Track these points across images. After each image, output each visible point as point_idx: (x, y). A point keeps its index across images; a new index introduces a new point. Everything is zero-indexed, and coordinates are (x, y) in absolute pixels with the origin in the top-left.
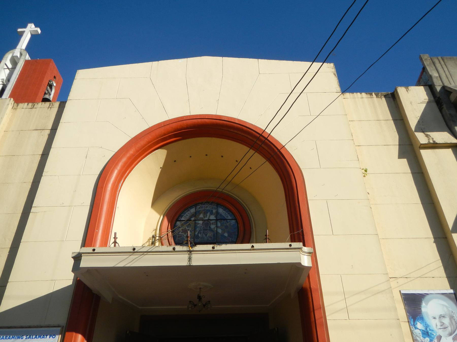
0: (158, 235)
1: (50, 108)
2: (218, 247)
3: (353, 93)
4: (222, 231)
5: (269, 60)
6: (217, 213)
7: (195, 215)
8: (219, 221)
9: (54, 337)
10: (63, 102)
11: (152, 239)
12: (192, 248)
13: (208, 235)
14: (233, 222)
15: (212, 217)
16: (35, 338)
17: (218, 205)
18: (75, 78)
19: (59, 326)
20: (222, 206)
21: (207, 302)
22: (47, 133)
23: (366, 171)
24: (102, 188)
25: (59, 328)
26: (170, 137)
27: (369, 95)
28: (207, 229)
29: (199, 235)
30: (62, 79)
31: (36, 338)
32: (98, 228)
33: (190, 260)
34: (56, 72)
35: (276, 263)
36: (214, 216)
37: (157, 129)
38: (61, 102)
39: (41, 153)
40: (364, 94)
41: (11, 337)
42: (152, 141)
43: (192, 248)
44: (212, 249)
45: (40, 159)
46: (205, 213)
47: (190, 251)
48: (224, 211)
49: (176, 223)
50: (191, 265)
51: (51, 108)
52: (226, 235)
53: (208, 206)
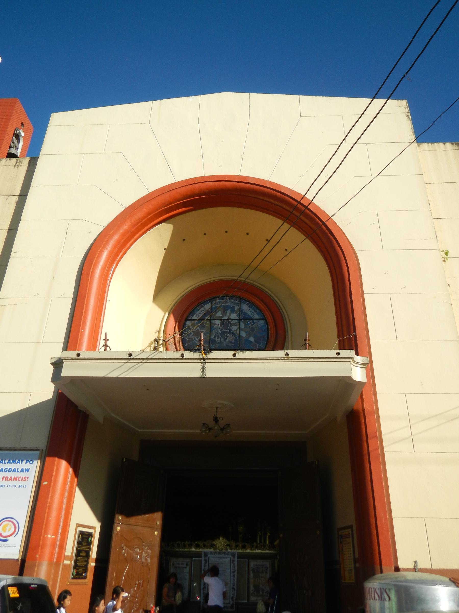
0: (162, 339)
1: (16, 167)
2: (240, 354)
3: (433, 144)
4: (246, 335)
5: (314, 97)
6: (240, 310)
7: (211, 312)
8: (242, 321)
9: (31, 462)
10: (33, 157)
11: (155, 343)
12: (206, 354)
13: (227, 340)
14: (262, 322)
15: (234, 316)
16: (8, 463)
17: (241, 299)
18: (49, 125)
19: (37, 450)
20: (247, 301)
21: (226, 425)
22: (15, 201)
23: (447, 254)
24: (88, 274)
25: (38, 452)
26: (177, 207)
27: (456, 146)
28: (228, 331)
29: (216, 339)
30: (32, 127)
31: (10, 463)
32: (84, 328)
33: (203, 370)
34: (24, 117)
35: (319, 376)
36: (236, 314)
37: (160, 195)
38: (31, 158)
39: (7, 227)
40: (448, 145)
42: (153, 212)
43: (206, 354)
44: (233, 357)
45: (6, 235)
46: (224, 310)
47: (204, 359)
48: (249, 308)
49: (185, 323)
50: (205, 376)
51: (18, 166)
52: (252, 339)
53: (228, 302)
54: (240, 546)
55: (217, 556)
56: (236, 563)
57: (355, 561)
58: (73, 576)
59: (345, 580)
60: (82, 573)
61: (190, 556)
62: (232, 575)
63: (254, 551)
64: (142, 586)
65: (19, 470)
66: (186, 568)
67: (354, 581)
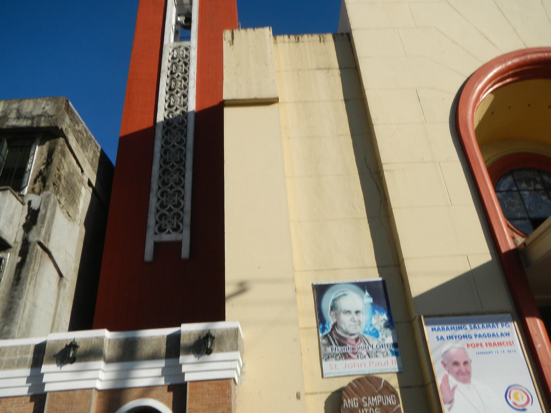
1: (322, 43)
29: (531, 208)
41: (450, 327)
65: (499, 334)
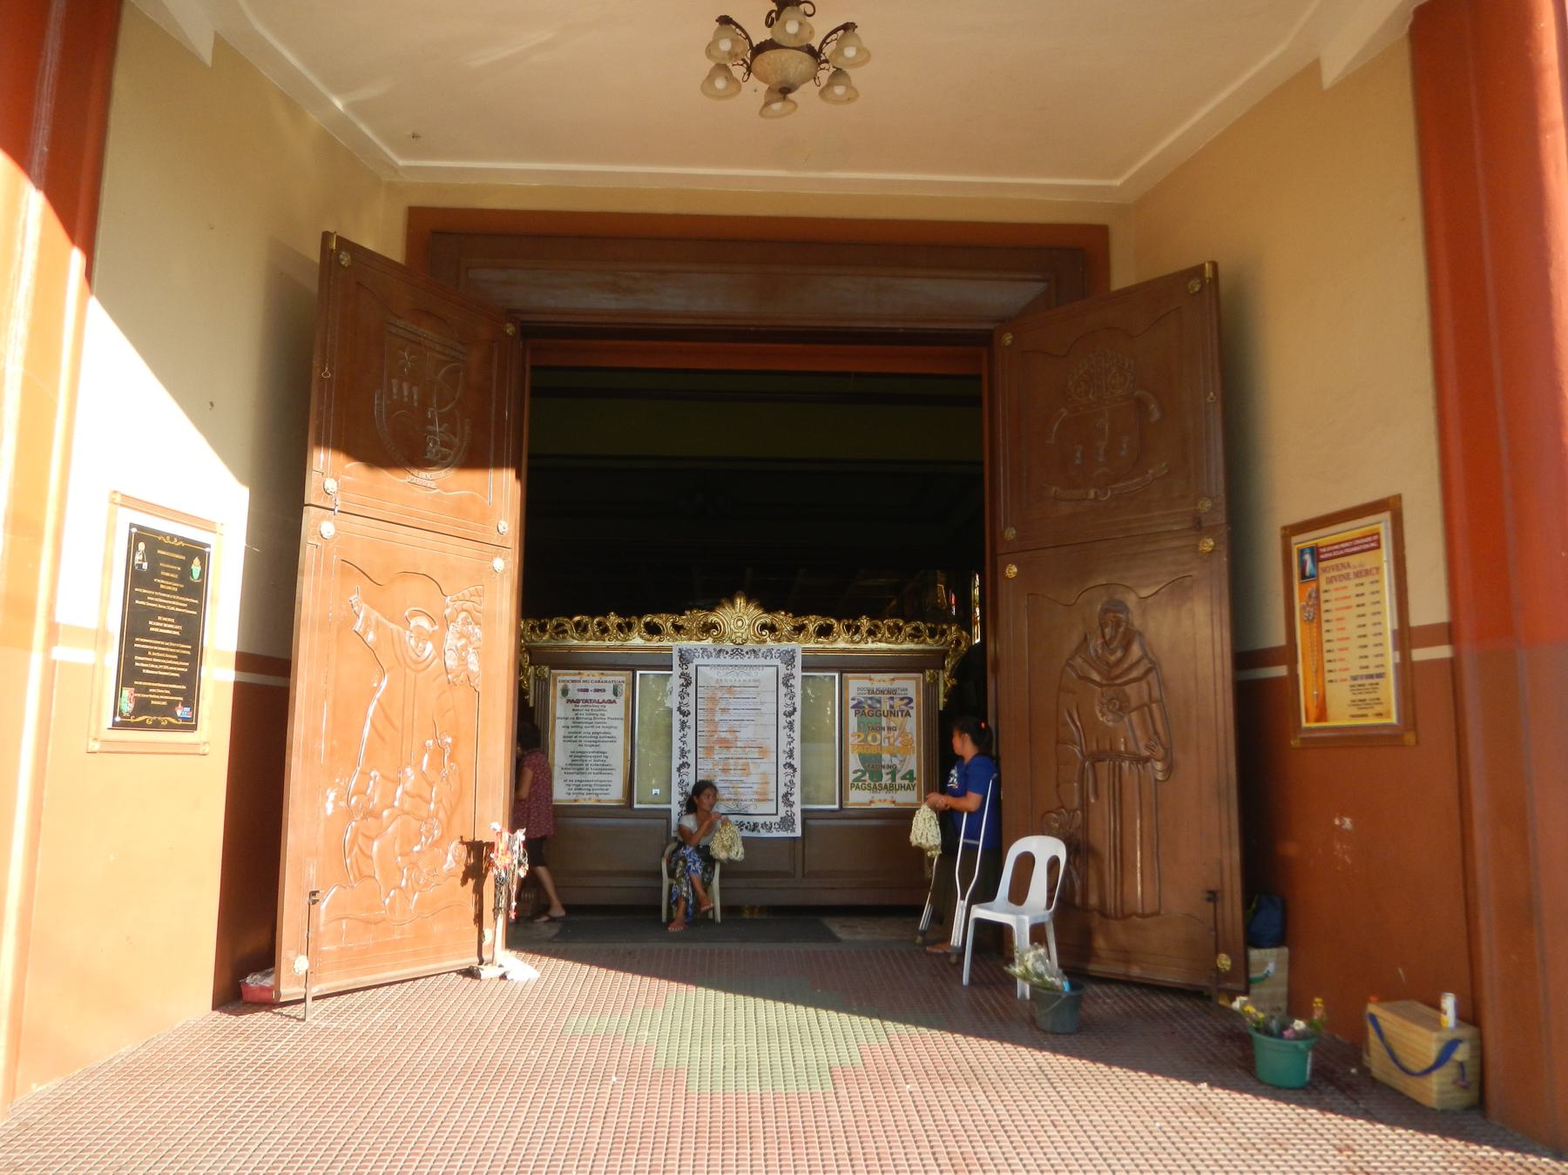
54: (811, 628)
55: (728, 660)
56: (797, 683)
57: (1406, 637)
58: (121, 714)
59: (1322, 715)
60: (172, 705)
61: (630, 663)
62: (783, 720)
63: (862, 646)
64: (451, 758)
66: (610, 702)
67: (1393, 719)
